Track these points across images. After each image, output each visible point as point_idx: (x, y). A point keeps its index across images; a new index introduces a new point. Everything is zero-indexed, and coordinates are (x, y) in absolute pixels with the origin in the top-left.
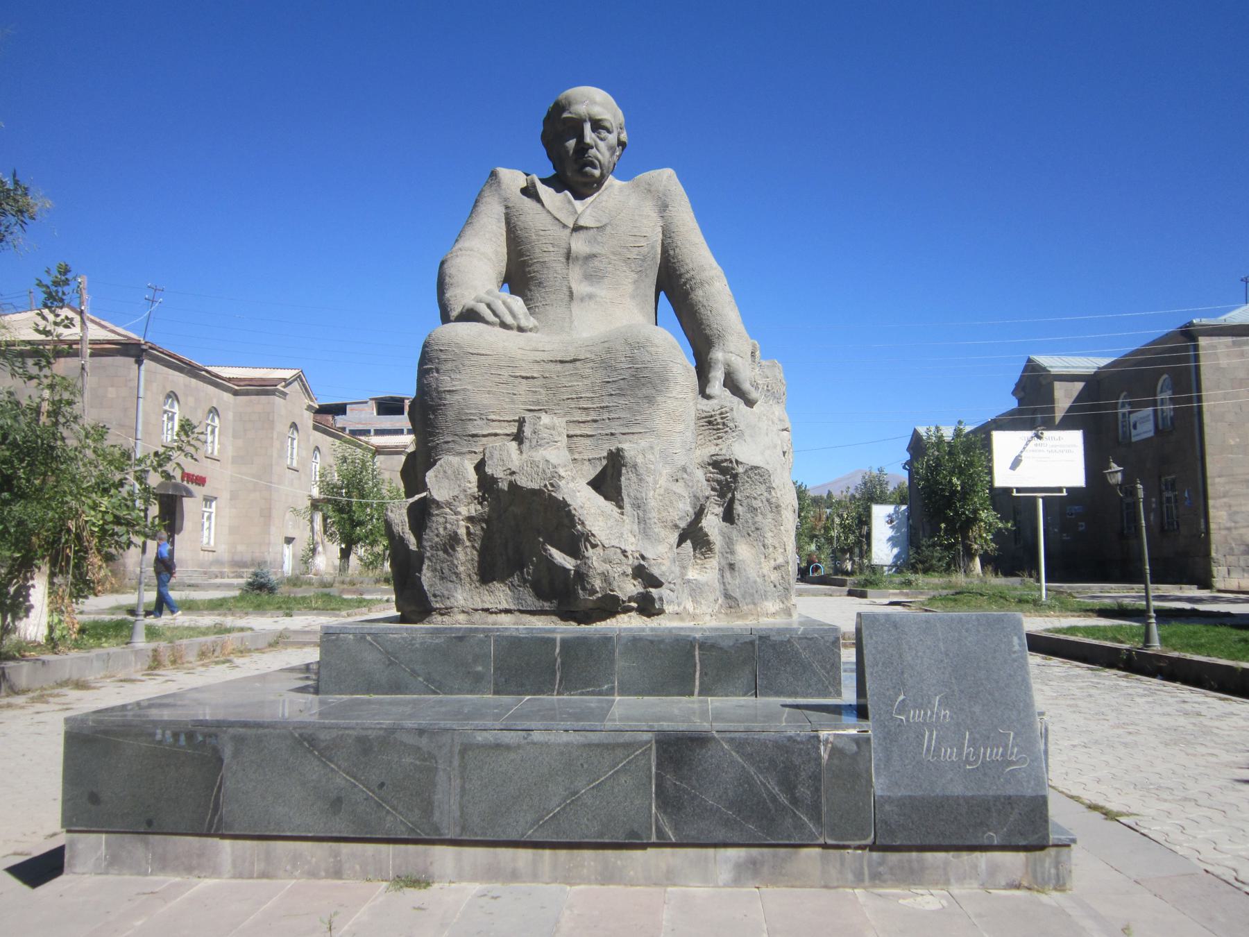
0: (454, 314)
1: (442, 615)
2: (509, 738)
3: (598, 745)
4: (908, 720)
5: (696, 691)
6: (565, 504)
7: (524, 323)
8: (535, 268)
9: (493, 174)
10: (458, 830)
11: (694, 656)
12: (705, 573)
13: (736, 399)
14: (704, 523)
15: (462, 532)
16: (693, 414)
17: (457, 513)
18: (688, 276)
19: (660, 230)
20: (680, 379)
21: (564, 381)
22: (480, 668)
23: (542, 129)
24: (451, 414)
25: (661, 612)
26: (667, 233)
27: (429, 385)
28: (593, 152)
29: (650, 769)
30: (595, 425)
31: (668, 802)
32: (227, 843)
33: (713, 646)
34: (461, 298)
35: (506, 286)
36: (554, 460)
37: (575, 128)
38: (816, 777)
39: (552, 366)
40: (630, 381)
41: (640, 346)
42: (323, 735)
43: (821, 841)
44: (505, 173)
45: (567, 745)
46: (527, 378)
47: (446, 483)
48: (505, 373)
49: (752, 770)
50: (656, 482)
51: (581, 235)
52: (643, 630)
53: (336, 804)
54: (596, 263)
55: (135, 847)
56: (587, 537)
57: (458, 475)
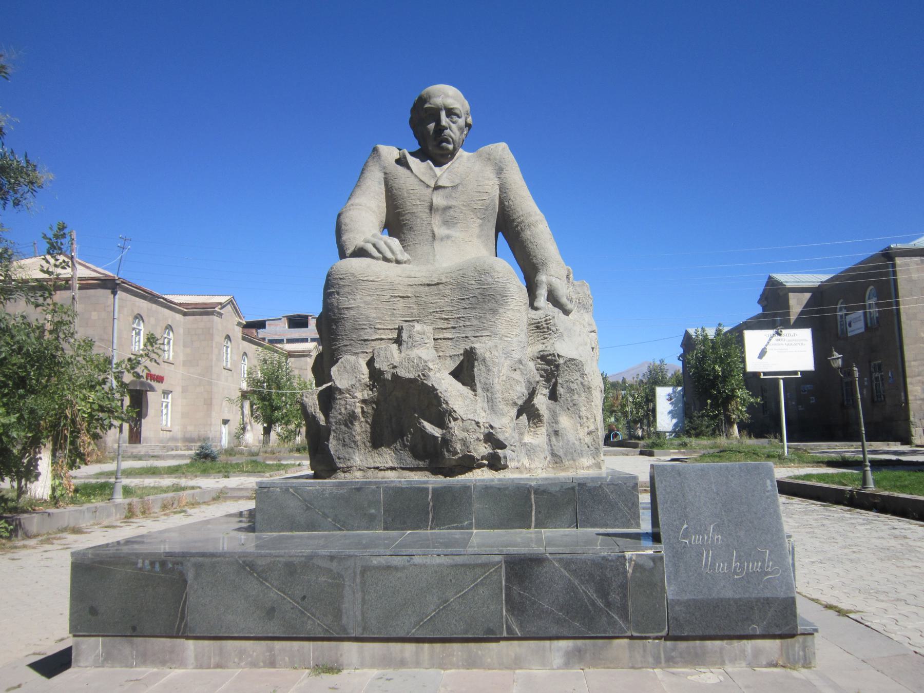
0: (349, 252)
1: (344, 472)
2: (397, 561)
3: (463, 565)
4: (690, 543)
5: (533, 525)
6: (433, 389)
7: (400, 257)
8: (407, 217)
9: (375, 150)
10: (360, 630)
11: (530, 499)
12: (537, 438)
13: (556, 310)
14: (535, 401)
15: (358, 411)
16: (525, 321)
17: (354, 397)
18: (519, 220)
20: (516, 296)
21: (431, 299)
22: (373, 511)
23: (409, 116)
24: (348, 325)
25: (505, 467)
26: (503, 189)
27: (332, 304)
28: (447, 132)
29: (501, 582)
30: (454, 331)
31: (515, 606)
32: (191, 643)
33: (544, 491)
34: (354, 240)
35: (386, 230)
36: (424, 357)
37: (434, 115)
38: (624, 587)
39: (422, 288)
40: (479, 297)
41: (486, 272)
42: (260, 562)
43: (629, 634)
44: (384, 149)
45: (439, 565)
46: (403, 297)
47: (346, 375)
48: (387, 294)
49: (576, 582)
50: (499, 372)
51: (441, 192)
52: (492, 480)
53: (271, 612)
54: (451, 212)
55: (124, 646)
56: (450, 413)
57: (355, 369)
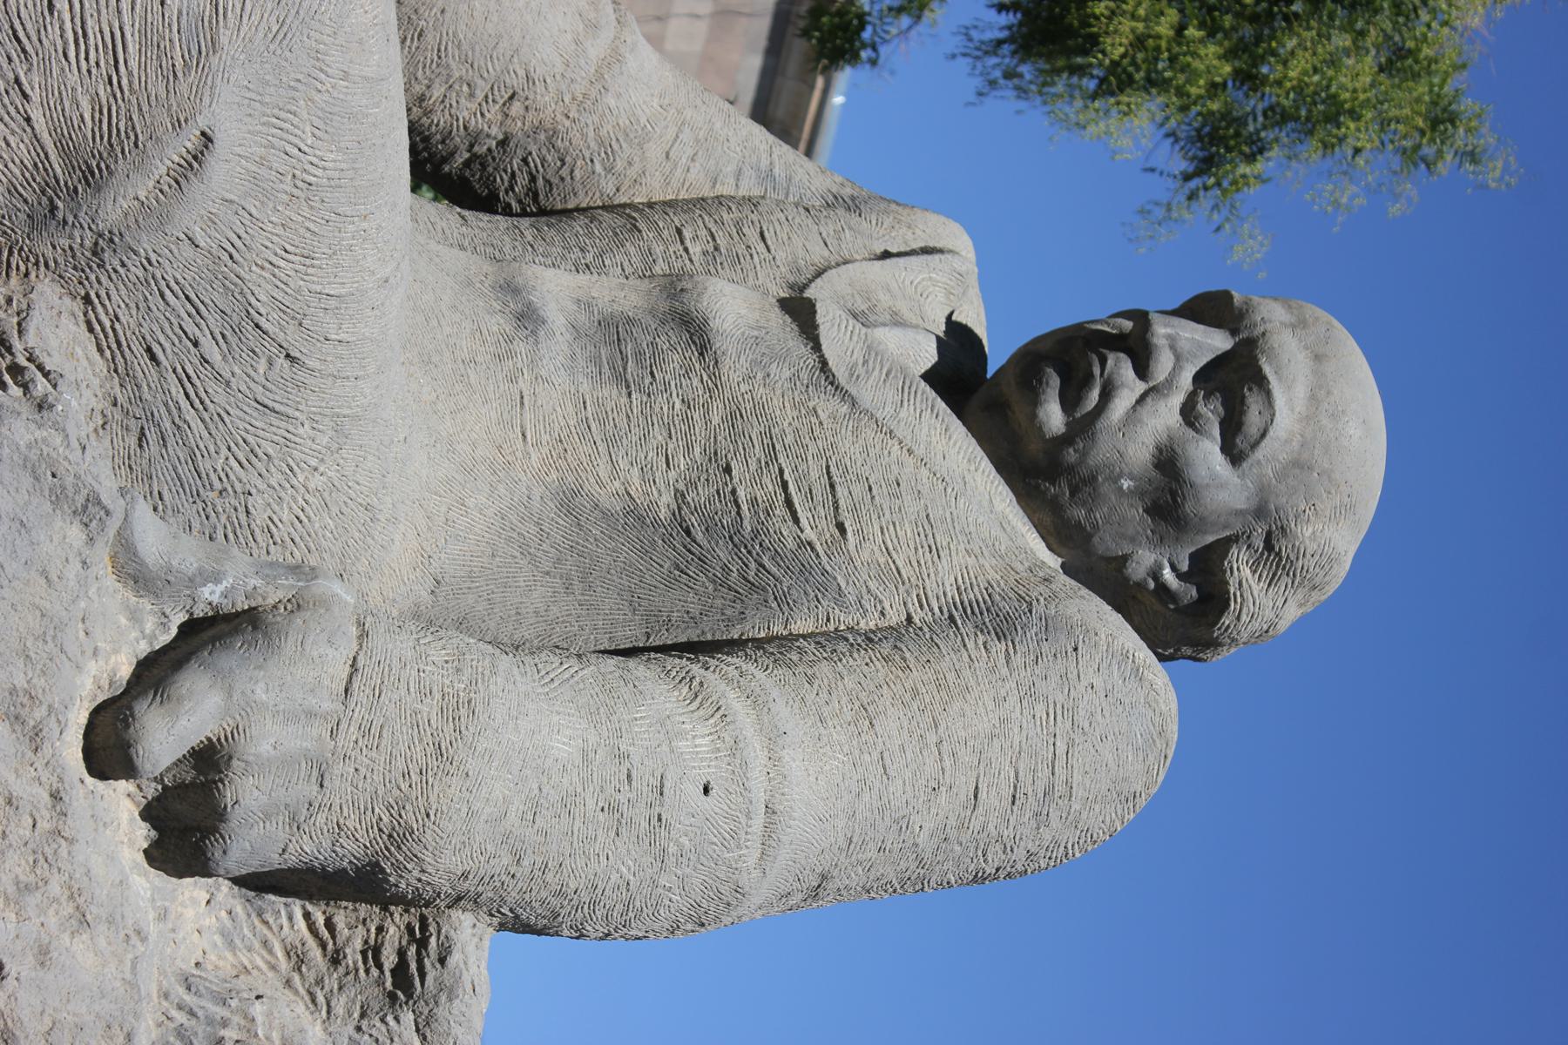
19: (895, 617)
28: (1130, 387)
